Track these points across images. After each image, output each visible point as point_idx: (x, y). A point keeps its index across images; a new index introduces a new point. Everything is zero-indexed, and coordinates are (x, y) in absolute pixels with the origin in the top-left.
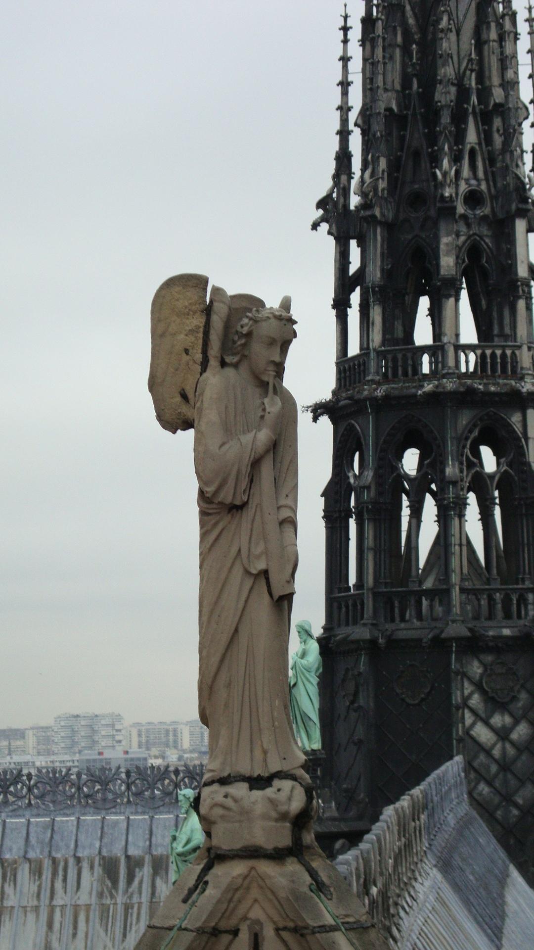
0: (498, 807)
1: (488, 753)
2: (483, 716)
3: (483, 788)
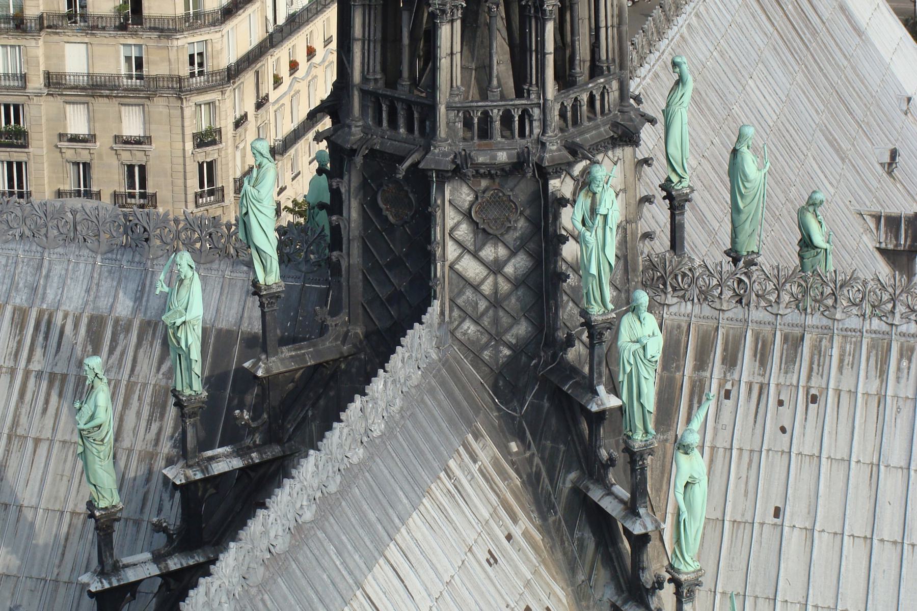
0: (485, 347)
1: (476, 288)
2: (472, 248)
3: (469, 327)
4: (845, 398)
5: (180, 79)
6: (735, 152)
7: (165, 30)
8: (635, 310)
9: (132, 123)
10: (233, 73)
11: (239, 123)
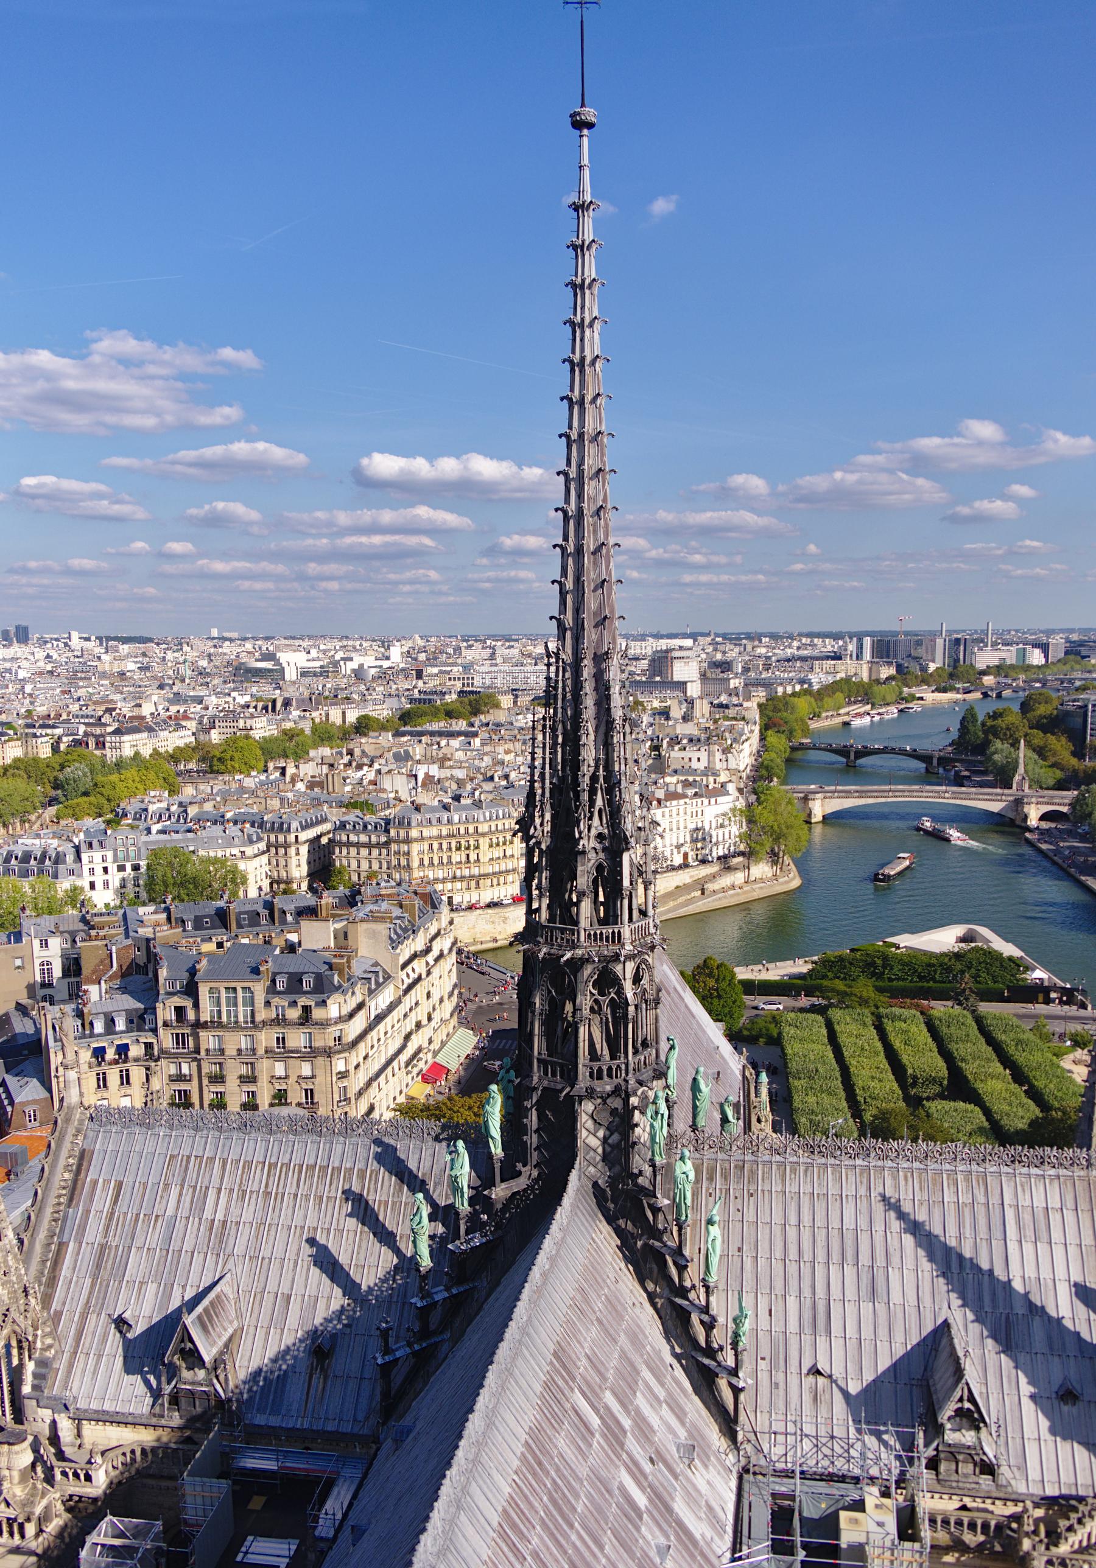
1: (595, 1151)
3: (592, 1169)
4: (766, 1193)
5: (330, 1048)
6: (695, 1079)
7: (324, 1024)
8: (682, 1159)
9: (306, 1069)
10: (355, 1043)
11: (357, 1067)
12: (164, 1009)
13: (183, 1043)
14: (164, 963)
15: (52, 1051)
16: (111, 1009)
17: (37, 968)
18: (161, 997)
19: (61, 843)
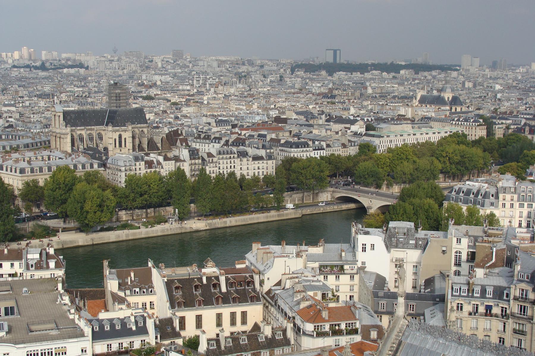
12: (515, 289)
13: (524, 312)
14: (519, 262)
15: (449, 301)
16: (486, 284)
17: (453, 254)
18: (515, 282)
19: (489, 186)
